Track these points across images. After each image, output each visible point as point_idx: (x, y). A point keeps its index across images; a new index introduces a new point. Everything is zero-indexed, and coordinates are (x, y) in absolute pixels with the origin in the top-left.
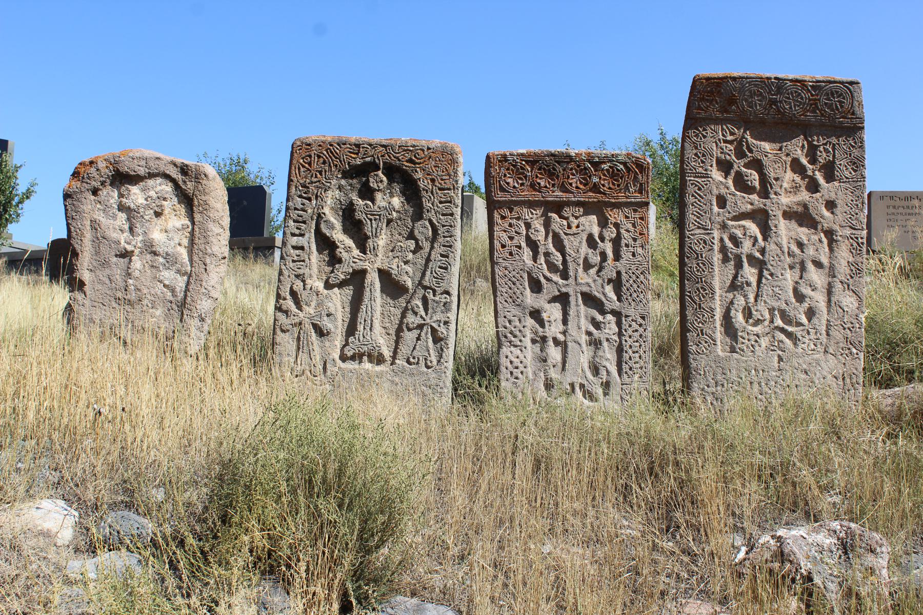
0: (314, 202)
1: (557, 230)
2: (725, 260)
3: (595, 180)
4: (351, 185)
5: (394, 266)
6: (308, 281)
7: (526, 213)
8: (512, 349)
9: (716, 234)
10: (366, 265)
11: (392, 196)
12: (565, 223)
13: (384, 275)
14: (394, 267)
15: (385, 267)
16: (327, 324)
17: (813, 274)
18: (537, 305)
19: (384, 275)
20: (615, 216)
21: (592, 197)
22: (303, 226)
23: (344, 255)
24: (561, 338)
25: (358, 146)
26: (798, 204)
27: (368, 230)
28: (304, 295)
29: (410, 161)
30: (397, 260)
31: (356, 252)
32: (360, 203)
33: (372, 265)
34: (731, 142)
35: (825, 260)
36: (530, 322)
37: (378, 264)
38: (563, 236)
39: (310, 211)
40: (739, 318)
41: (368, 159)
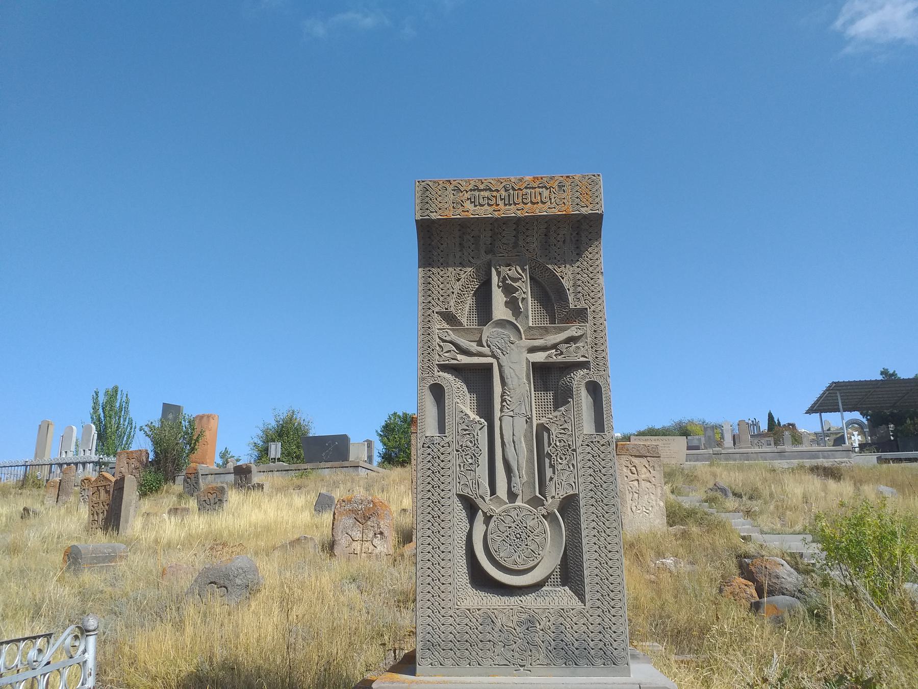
17: (652, 497)
40: (634, 509)
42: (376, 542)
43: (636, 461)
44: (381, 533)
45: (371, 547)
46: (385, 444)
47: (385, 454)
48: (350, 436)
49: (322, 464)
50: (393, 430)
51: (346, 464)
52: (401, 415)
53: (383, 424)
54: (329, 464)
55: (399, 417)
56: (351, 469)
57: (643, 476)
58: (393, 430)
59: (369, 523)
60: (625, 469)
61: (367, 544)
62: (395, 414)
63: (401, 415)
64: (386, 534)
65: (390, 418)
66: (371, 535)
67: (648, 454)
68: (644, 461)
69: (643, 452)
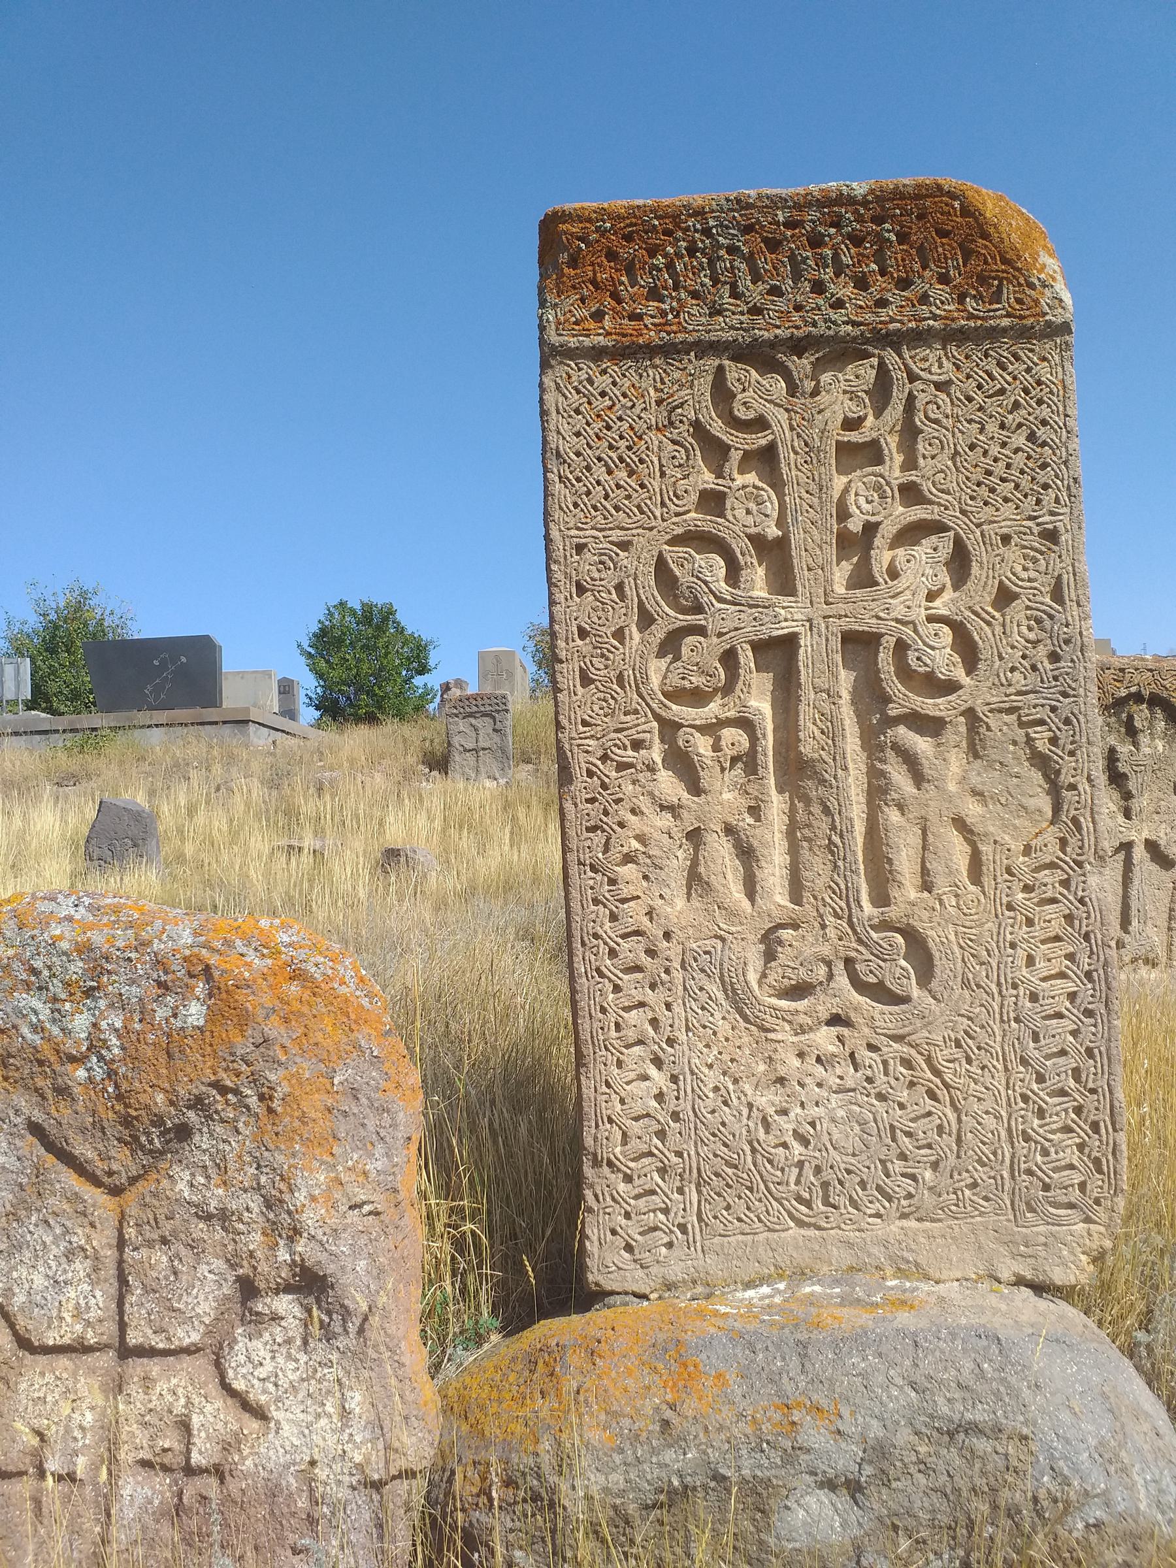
4: (1108, 725)
10: (1133, 836)
11: (1153, 739)
13: (1152, 846)
14: (1162, 835)
19: (1152, 846)
25: (1122, 670)
27: (1132, 785)
30: (1164, 826)
31: (1121, 819)
32: (1124, 749)
33: (1138, 834)
37: (1145, 834)
41: (1133, 689)
42: (257, 1361)
44: (310, 1283)
45: (212, 1417)
46: (320, 675)
47: (323, 698)
48: (218, 639)
49: (143, 717)
50: (340, 641)
51: (211, 714)
52: (358, 607)
53: (315, 628)
54: (162, 716)
55: (353, 612)
56: (227, 730)
58: (340, 641)
59: (182, 1183)
61: (175, 1387)
62: (342, 604)
63: (358, 607)
64: (356, 1281)
65: (331, 614)
66: (205, 1295)
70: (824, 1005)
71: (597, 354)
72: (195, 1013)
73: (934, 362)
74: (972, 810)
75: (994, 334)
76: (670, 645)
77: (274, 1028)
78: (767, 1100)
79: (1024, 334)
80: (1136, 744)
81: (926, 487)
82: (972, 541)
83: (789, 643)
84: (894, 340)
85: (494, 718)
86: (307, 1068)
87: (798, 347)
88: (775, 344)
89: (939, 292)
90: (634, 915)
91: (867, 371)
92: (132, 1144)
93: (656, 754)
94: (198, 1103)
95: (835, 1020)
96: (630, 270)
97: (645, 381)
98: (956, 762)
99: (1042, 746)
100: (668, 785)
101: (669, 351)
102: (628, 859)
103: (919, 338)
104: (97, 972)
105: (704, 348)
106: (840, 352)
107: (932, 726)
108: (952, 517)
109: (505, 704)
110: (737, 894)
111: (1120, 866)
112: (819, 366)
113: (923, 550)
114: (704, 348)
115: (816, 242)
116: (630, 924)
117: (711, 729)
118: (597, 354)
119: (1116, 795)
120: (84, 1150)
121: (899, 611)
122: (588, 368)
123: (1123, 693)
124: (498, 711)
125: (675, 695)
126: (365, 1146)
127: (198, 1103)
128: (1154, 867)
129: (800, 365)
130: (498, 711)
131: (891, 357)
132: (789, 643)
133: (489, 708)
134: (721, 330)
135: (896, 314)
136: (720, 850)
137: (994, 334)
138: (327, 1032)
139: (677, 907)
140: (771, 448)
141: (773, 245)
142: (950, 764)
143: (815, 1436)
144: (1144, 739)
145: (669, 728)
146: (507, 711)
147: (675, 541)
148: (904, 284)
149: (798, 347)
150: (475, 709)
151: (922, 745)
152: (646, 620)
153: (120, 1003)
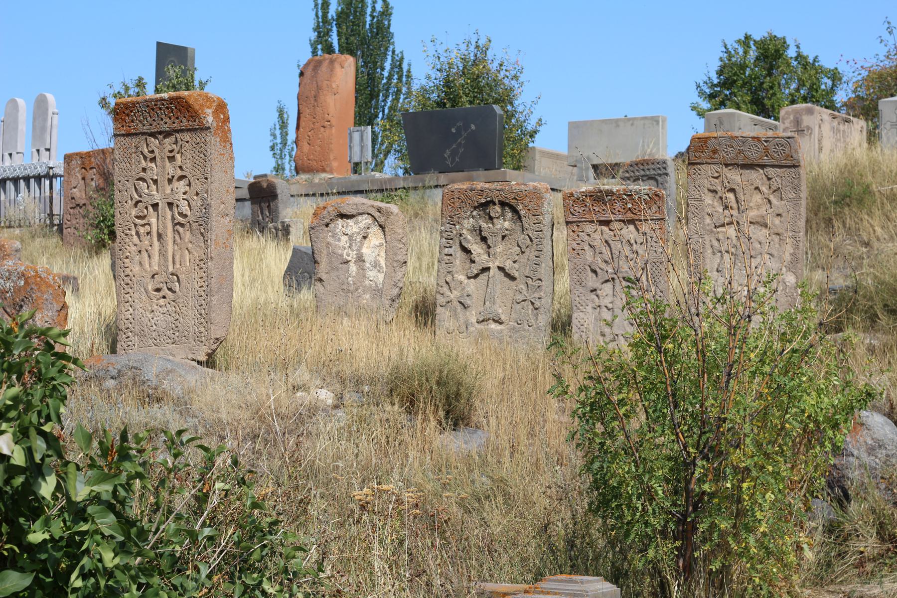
0: (458, 227)
1: (607, 239)
2: (714, 253)
3: (630, 206)
5: (508, 265)
6: (456, 275)
7: (589, 228)
8: (581, 314)
9: (706, 237)
12: (612, 233)
15: (501, 266)
16: (468, 302)
18: (595, 286)
20: (644, 227)
21: (630, 216)
22: (451, 242)
23: (477, 259)
24: (610, 306)
26: (758, 216)
28: (452, 285)
29: (515, 199)
34: (716, 178)
35: (775, 253)
36: (593, 296)
37: (497, 264)
38: (611, 242)
39: (455, 232)
43: (735, 176)
57: (753, 214)
60: (708, 199)
67: (766, 160)
68: (756, 176)
69: (753, 155)
70: (162, 294)
71: (123, 135)
72: (22, 283)
73: (187, 136)
74: (190, 246)
75: (196, 129)
76: (136, 205)
77: (33, 286)
78: (150, 316)
79: (202, 129)
80: (493, 223)
81: (184, 167)
82: (192, 180)
83: (157, 204)
84: (178, 131)
85: (657, 181)
86: (39, 294)
87: (160, 133)
88: (155, 133)
89: (184, 120)
90: (128, 271)
91: (173, 139)
92: (15, 309)
93: (133, 233)
94: (23, 300)
95: (164, 297)
96: (128, 115)
97: (135, 141)
98: (188, 234)
99: (202, 231)
100: (135, 238)
101: (136, 134)
102: (127, 258)
103: (182, 131)
104: (10, 275)
105: (143, 134)
106: (167, 134)
107: (182, 225)
108: (189, 176)
109: (665, 168)
110: (148, 266)
111: (486, 278)
112: (165, 137)
113: (182, 183)
114: (143, 134)
115: (160, 109)
116: (126, 273)
117: (143, 226)
118: (123, 135)
119: (485, 246)
120: (8, 310)
121: (177, 197)
122: (122, 139)
123: (483, 201)
124: (660, 175)
125: (137, 217)
126: (48, 310)
127: (23, 300)
128: (506, 279)
129: (160, 137)
130: (660, 175)
131: (178, 135)
132: (157, 204)
133: (653, 172)
134: (146, 129)
135: (176, 126)
136: (145, 255)
137: (196, 129)
138: (43, 288)
139: (136, 269)
140: (155, 158)
141: (153, 110)
142: (188, 236)
143: (110, 368)
144: (495, 221)
145: (136, 225)
146: (667, 174)
147: (137, 180)
148: (177, 118)
149: (160, 133)
150: (642, 173)
151: (181, 230)
152: (132, 199)
153: (13, 281)
